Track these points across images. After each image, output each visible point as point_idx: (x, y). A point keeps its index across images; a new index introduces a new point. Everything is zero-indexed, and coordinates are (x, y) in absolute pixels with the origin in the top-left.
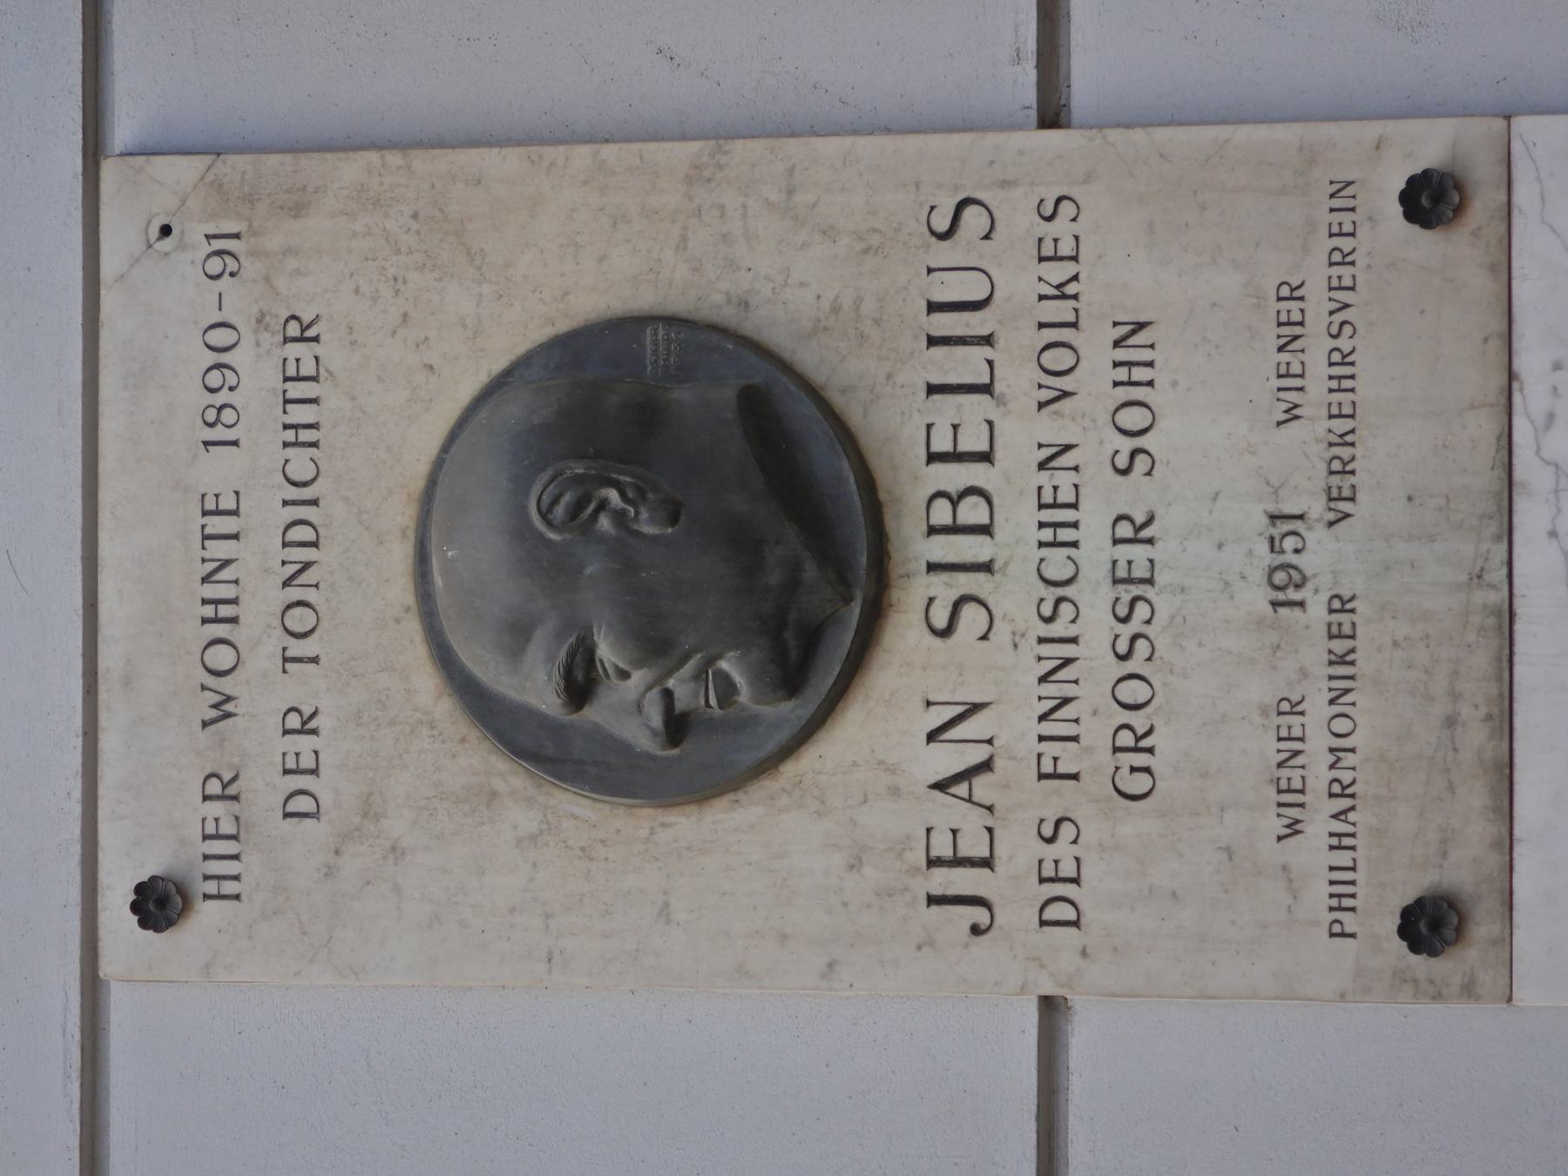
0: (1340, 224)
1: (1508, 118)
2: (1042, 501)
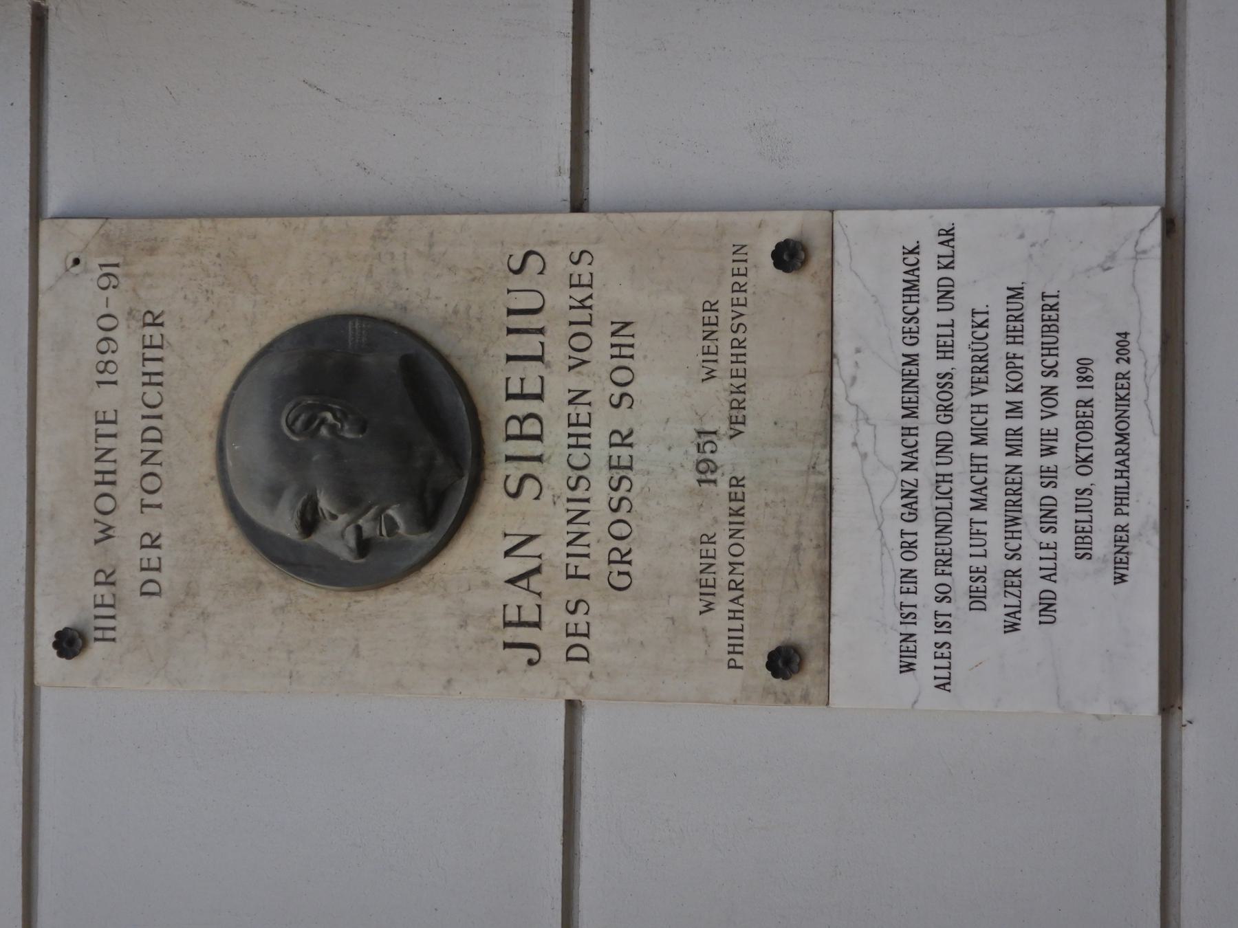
0: (738, 269)
1: (832, 211)
2: (570, 422)
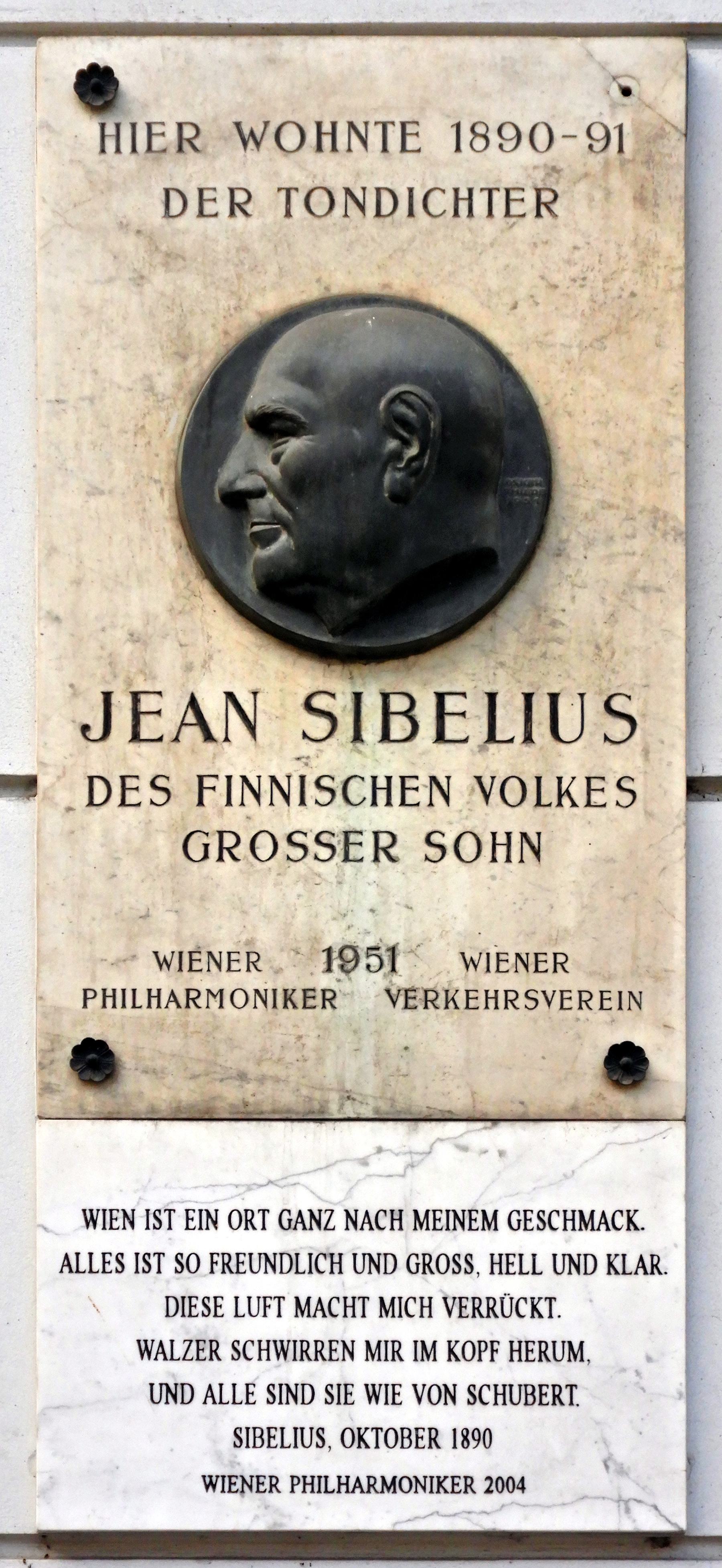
0: (610, 999)
1: (684, 1119)
